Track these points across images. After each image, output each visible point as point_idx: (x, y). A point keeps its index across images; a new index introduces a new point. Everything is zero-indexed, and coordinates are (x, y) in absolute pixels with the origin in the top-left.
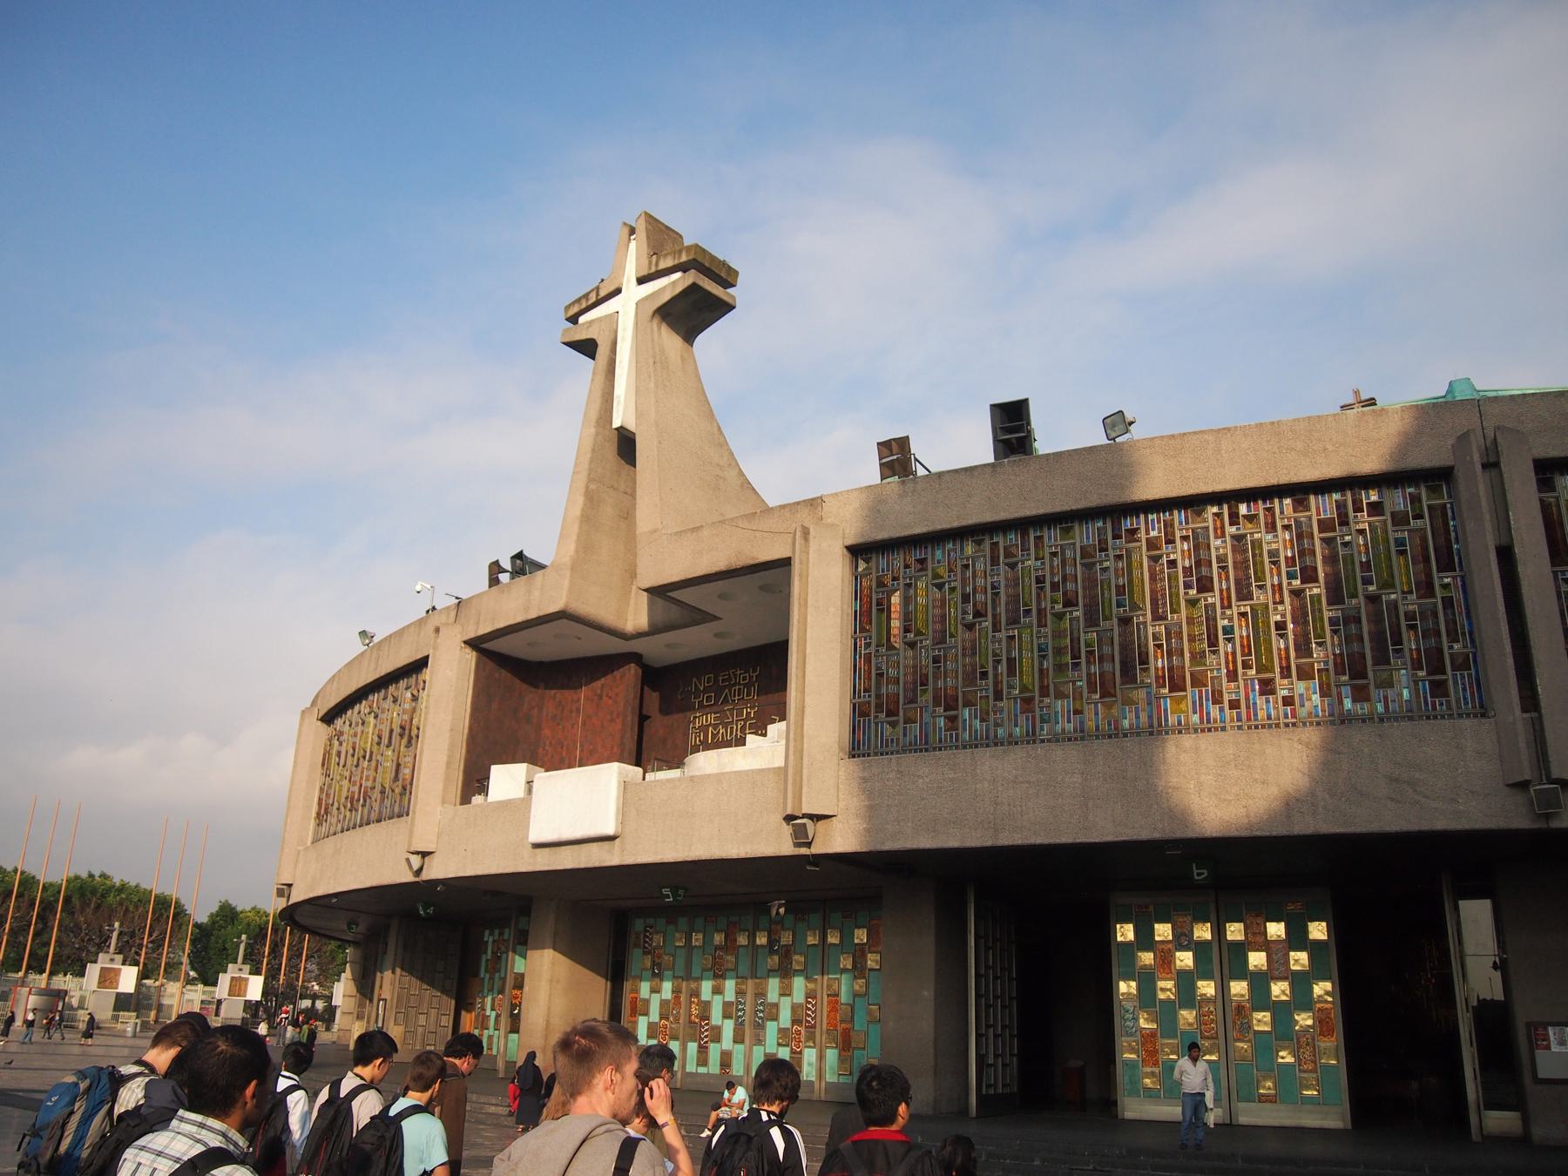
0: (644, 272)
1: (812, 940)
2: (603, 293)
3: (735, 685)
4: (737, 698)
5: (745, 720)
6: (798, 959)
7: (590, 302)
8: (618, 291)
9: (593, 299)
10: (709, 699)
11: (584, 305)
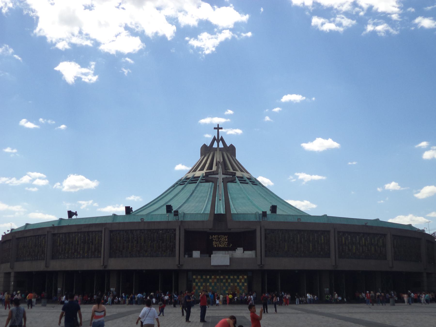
0: (224, 173)
1: (232, 277)
2: (215, 173)
3: (222, 238)
4: (223, 240)
5: (225, 244)
6: (229, 281)
7: (211, 174)
8: (218, 174)
9: (212, 173)
10: (217, 240)
11: (210, 174)
